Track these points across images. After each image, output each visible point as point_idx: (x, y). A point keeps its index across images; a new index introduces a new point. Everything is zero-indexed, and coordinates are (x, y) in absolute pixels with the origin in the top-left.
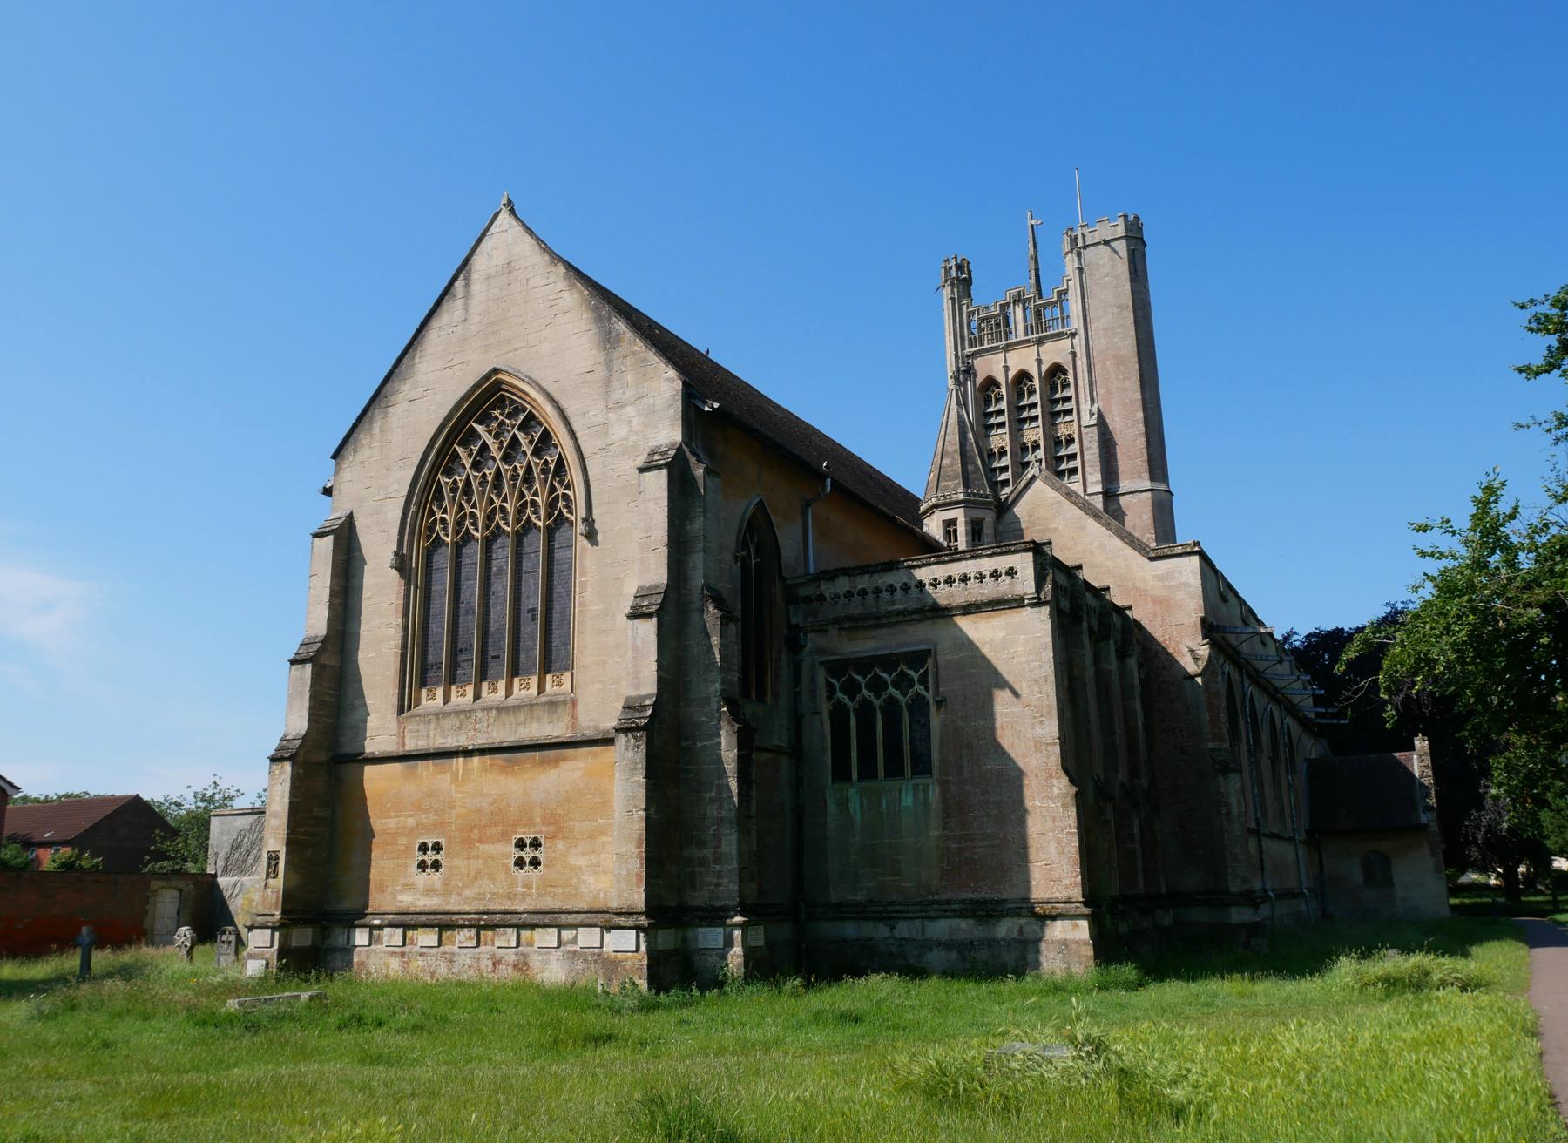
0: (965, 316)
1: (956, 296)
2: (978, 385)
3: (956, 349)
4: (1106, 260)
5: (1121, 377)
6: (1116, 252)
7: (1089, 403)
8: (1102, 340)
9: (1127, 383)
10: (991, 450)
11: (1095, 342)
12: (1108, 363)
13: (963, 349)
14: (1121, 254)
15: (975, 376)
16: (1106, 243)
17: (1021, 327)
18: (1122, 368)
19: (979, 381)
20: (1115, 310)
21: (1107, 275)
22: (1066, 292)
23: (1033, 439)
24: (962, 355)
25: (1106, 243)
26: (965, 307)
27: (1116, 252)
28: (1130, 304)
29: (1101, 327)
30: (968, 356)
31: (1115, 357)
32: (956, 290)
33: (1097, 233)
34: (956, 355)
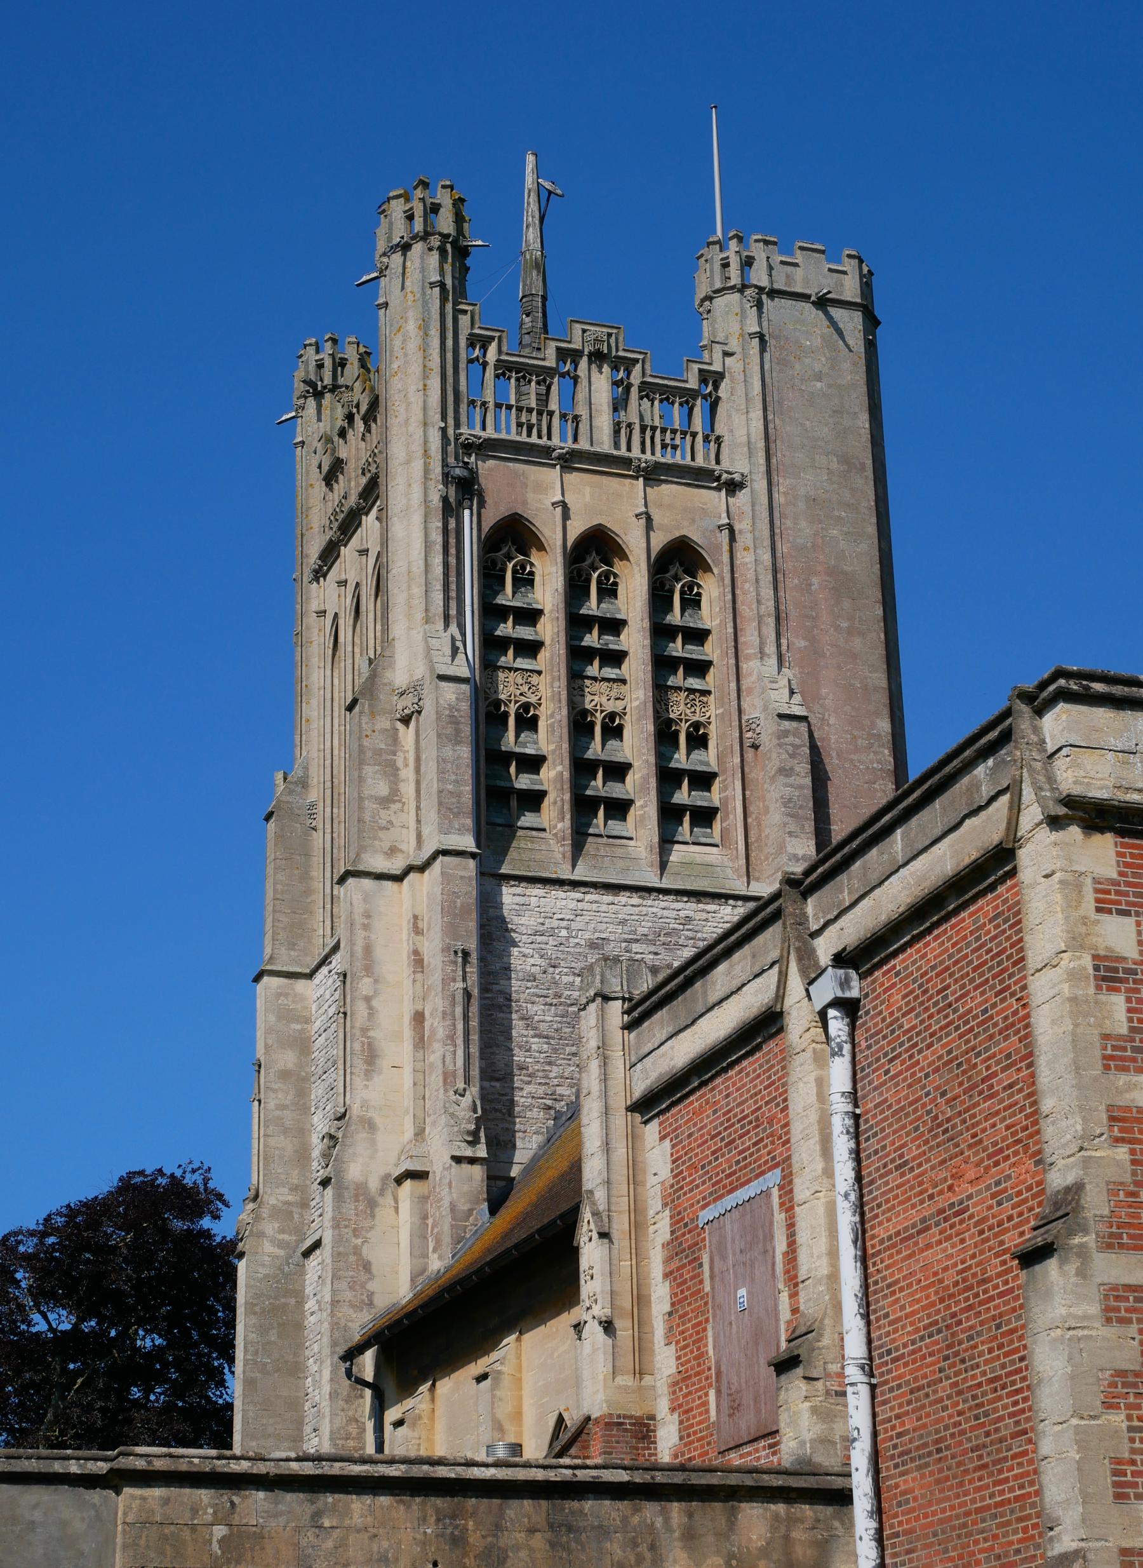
0: (463, 343)
1: (449, 282)
2: (486, 528)
3: (444, 417)
4: (818, 342)
5: (845, 625)
6: (840, 334)
7: (773, 661)
8: (803, 524)
9: (857, 643)
10: (498, 703)
11: (789, 523)
12: (815, 581)
13: (457, 425)
14: (851, 343)
15: (482, 504)
16: (823, 303)
17: (604, 422)
18: (847, 604)
19: (491, 517)
20: (835, 465)
21: (819, 377)
22: (718, 377)
23: (610, 706)
24: (457, 437)
25: (823, 303)
26: (464, 320)
27: (840, 334)
28: (869, 462)
29: (802, 492)
30: (468, 447)
31: (831, 572)
32: (448, 268)
33: (799, 273)
34: (444, 430)
